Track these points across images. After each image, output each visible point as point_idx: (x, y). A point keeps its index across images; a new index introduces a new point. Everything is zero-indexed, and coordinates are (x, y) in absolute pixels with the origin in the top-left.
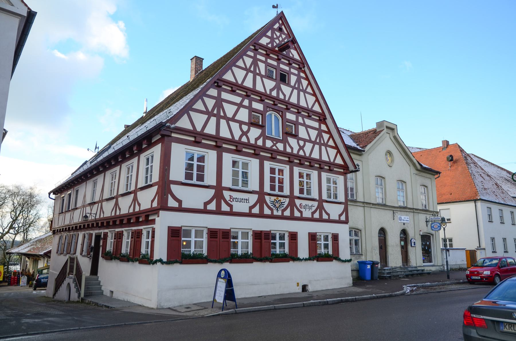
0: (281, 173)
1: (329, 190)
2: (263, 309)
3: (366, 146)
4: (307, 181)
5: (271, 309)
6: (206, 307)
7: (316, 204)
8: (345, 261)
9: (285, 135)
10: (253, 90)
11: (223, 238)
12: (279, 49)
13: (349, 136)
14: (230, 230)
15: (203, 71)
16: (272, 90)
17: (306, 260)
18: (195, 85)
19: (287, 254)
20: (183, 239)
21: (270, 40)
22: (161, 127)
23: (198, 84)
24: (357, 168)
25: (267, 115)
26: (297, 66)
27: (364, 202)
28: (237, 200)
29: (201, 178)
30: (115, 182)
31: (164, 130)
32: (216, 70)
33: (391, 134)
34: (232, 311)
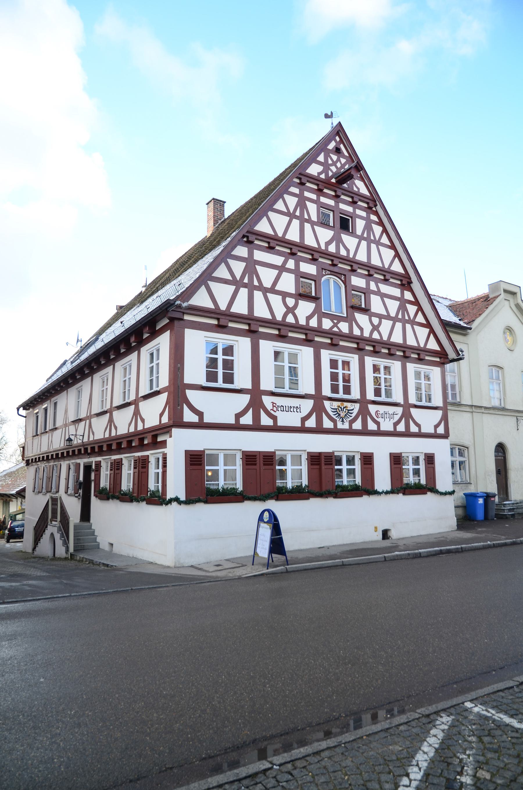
0: (346, 367)
1: (418, 388)
2: (326, 565)
3: (473, 321)
4: (386, 376)
5: (337, 566)
6: (244, 564)
7: (399, 411)
8: (445, 494)
9: (350, 310)
10: (301, 245)
11: (264, 465)
12: (337, 180)
13: (447, 306)
14: (274, 453)
15: (225, 220)
16: (328, 244)
17: (387, 493)
18: (215, 242)
19: (359, 486)
20: (207, 468)
21: (323, 167)
22: (169, 307)
23: (219, 241)
24: (460, 355)
25: (322, 281)
26: (365, 205)
27: (472, 406)
28: (283, 408)
29: (229, 378)
30: (107, 389)
31: (172, 310)
32: (244, 218)
33: (512, 300)
34: (281, 569)
